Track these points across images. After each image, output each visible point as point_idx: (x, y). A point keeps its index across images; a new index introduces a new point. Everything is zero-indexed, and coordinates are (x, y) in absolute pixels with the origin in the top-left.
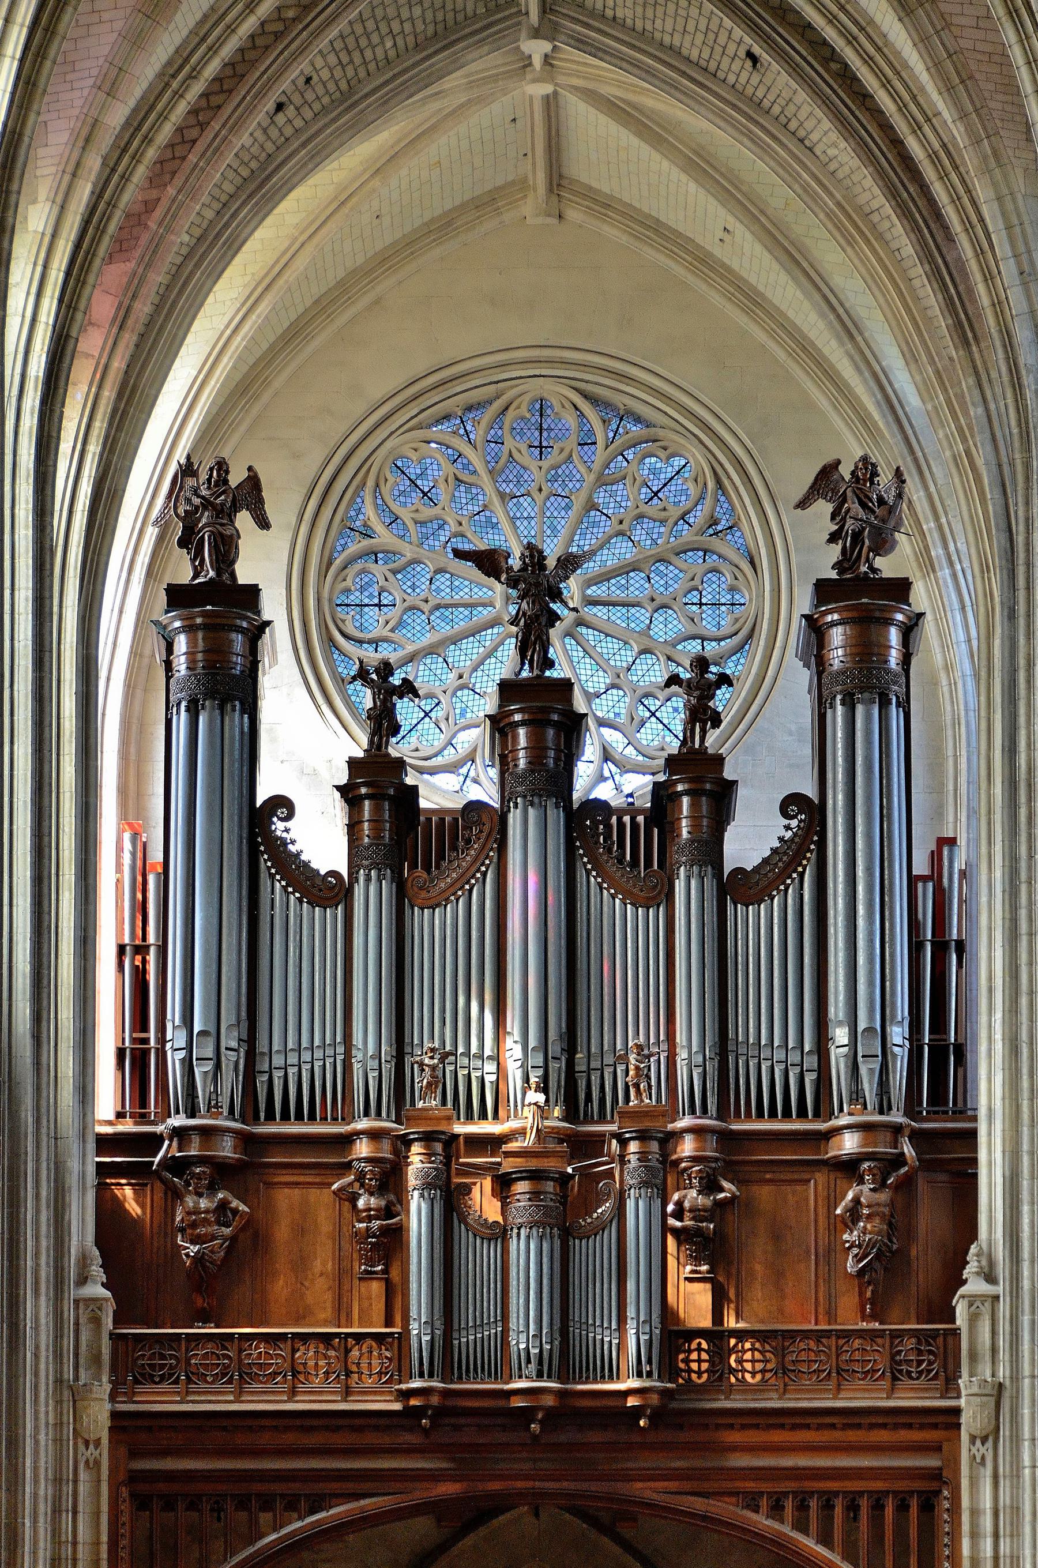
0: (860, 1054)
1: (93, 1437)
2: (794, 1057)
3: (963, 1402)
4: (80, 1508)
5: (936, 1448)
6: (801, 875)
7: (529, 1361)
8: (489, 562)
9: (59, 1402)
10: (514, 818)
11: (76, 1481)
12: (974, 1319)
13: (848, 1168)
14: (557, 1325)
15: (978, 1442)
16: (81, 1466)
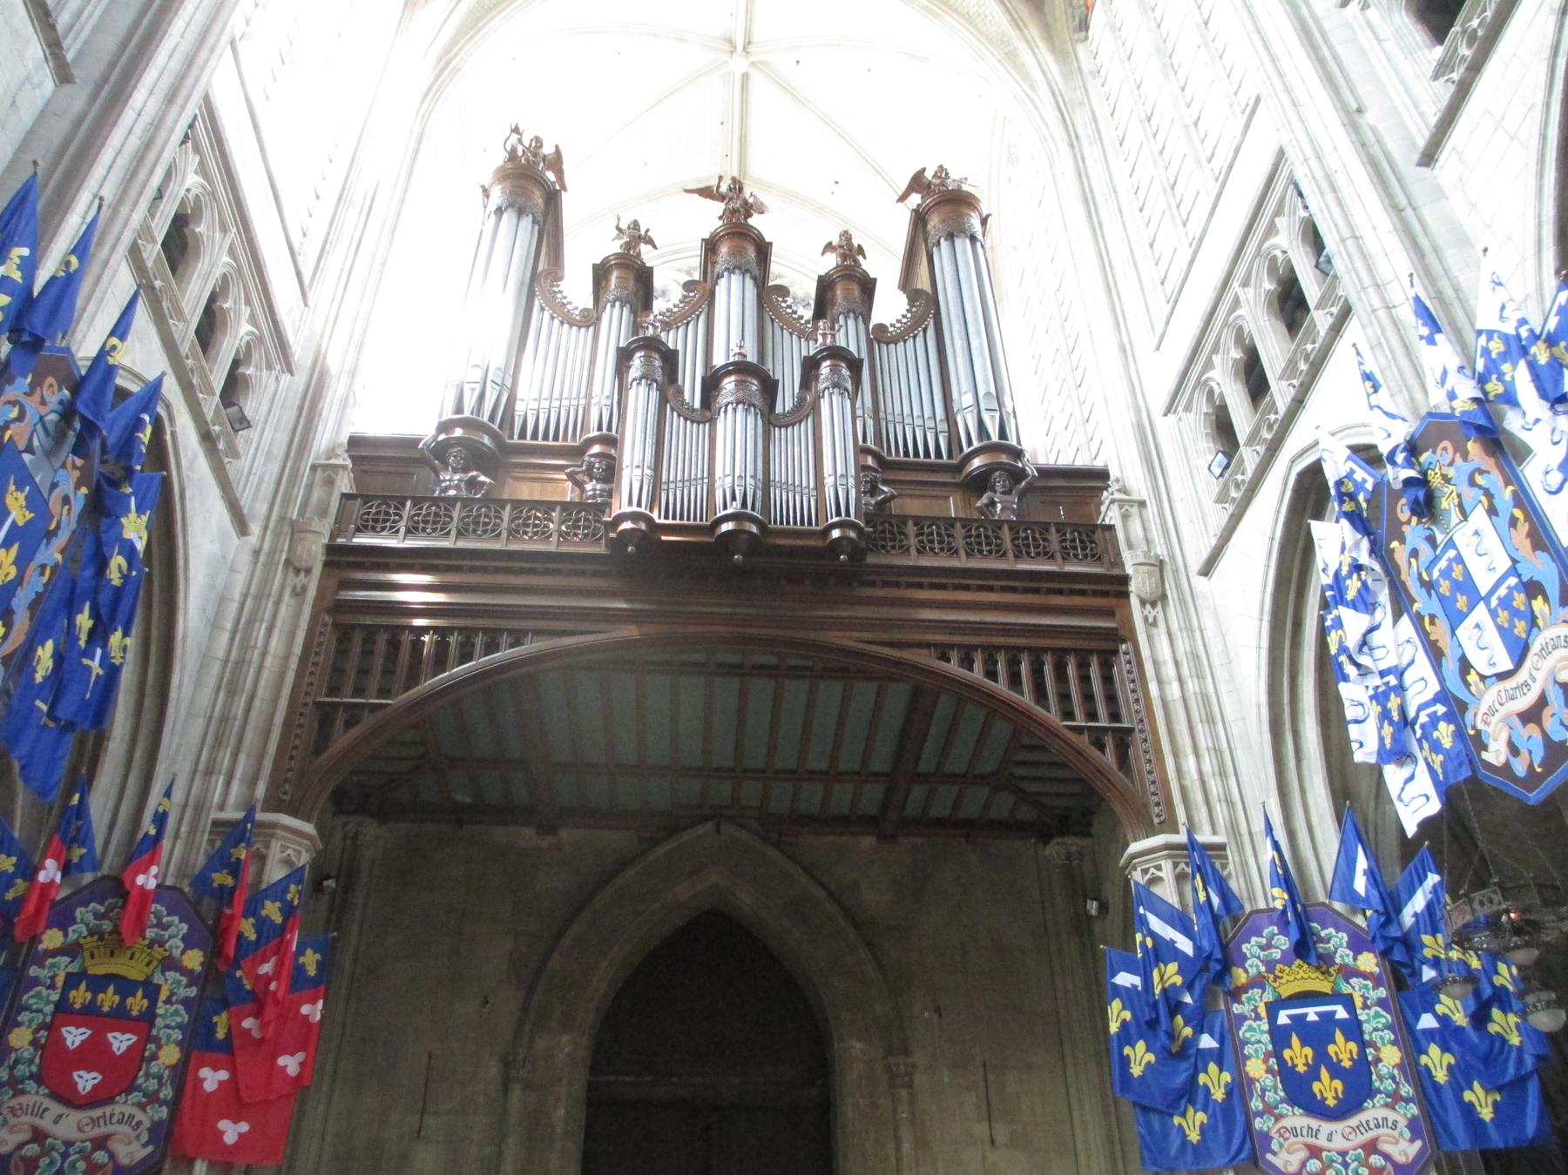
0: (983, 407)
1: (304, 565)
2: (930, 424)
3: (1129, 570)
4: (279, 623)
5: (1110, 613)
6: (925, 330)
7: (734, 498)
8: (706, 192)
9: (277, 534)
10: (721, 289)
11: (277, 604)
12: (1125, 517)
13: (980, 483)
14: (760, 475)
15: (1148, 607)
16: (288, 592)
